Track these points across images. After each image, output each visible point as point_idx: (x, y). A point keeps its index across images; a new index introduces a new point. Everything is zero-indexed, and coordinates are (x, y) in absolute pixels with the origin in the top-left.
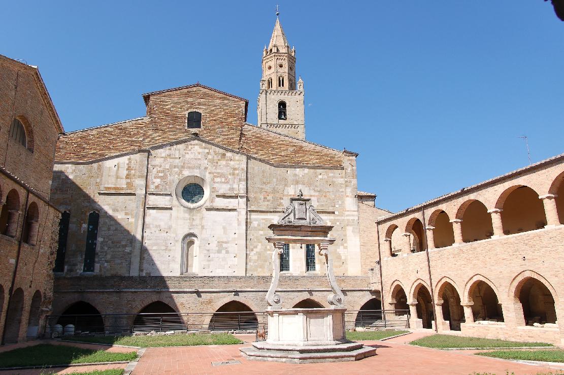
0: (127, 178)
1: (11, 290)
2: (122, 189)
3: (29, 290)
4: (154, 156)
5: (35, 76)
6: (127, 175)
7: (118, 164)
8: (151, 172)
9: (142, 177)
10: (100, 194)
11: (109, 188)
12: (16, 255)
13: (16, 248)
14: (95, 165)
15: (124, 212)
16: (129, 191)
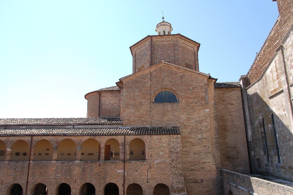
0: (278, 79)
1: (124, 185)
2: (277, 89)
3: (147, 184)
4: (285, 49)
5: (165, 65)
6: (277, 75)
7: (272, 70)
8: (287, 65)
9: (282, 74)
10: (271, 98)
11: (271, 92)
12: (123, 168)
13: (123, 165)
14: (264, 77)
15: (282, 109)
16: (281, 90)
